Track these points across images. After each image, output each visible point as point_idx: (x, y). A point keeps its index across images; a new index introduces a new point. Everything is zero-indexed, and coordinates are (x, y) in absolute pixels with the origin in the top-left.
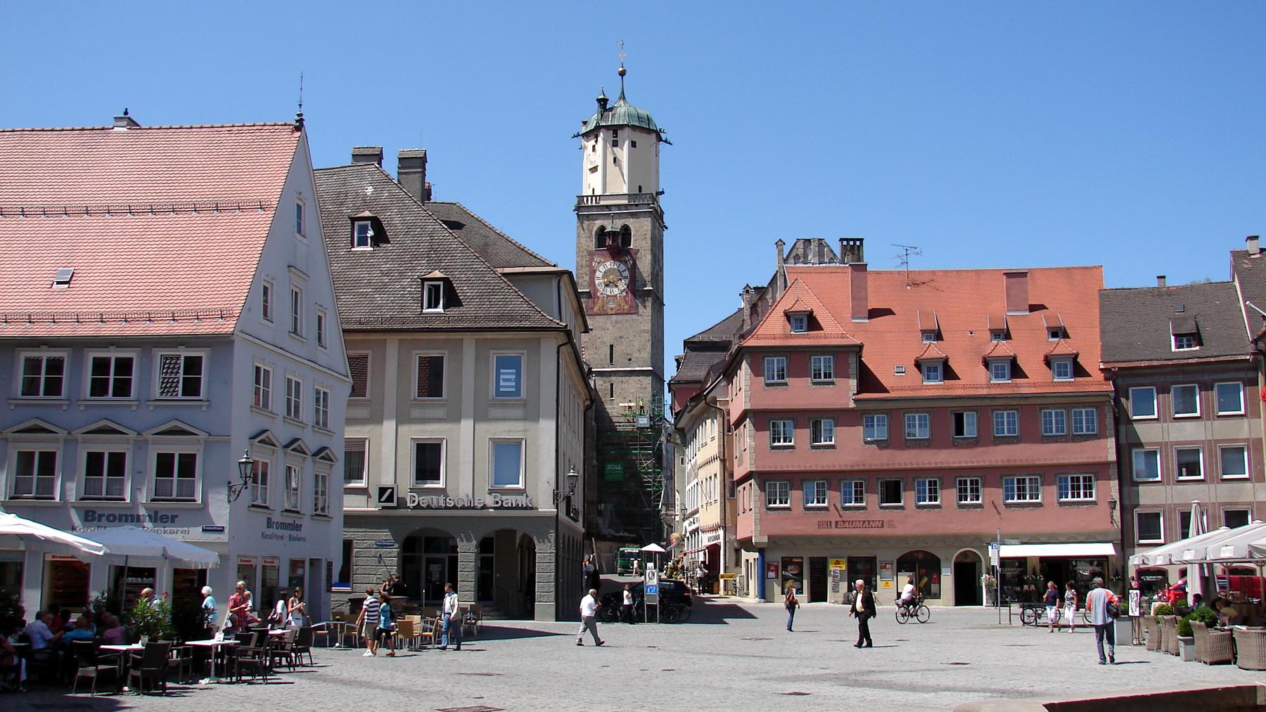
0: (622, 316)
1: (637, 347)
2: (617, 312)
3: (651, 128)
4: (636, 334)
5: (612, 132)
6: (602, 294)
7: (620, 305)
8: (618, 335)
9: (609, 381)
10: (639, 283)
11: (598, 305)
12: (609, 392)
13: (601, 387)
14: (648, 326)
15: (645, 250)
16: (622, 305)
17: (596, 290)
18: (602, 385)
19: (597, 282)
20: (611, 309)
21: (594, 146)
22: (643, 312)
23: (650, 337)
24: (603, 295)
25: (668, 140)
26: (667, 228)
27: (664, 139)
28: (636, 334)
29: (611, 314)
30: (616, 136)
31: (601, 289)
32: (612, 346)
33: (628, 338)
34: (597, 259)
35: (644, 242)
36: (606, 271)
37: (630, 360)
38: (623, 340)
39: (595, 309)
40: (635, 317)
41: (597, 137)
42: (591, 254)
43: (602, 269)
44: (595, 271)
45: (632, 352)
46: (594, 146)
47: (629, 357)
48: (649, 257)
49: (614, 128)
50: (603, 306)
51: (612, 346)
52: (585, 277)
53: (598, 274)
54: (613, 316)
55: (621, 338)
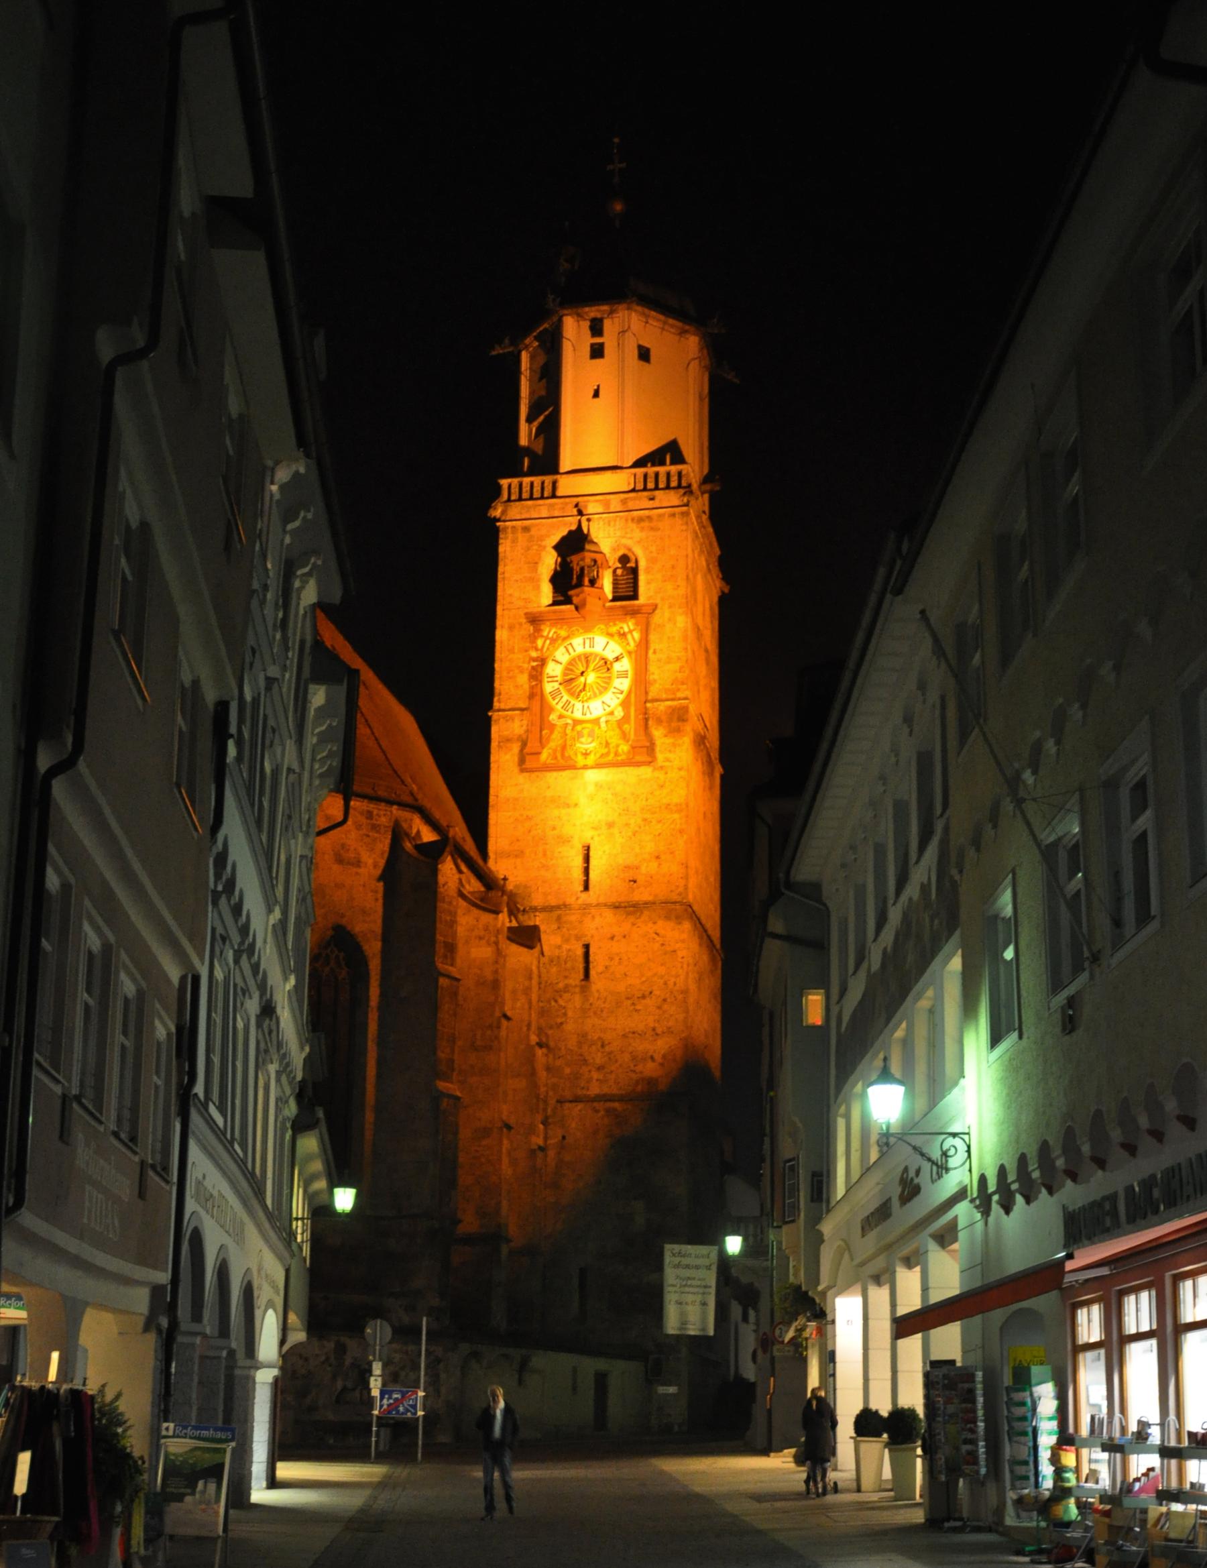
5: (586, 325)
6: (561, 717)
7: (607, 744)
9: (578, 938)
10: (657, 686)
11: (552, 744)
13: (557, 952)
17: (545, 709)
18: (559, 947)
19: (549, 687)
20: (586, 754)
22: (667, 760)
24: (562, 721)
29: (585, 767)
34: (548, 631)
36: (574, 660)
39: (545, 755)
43: (562, 655)
44: (543, 662)
50: (564, 748)
53: (553, 670)
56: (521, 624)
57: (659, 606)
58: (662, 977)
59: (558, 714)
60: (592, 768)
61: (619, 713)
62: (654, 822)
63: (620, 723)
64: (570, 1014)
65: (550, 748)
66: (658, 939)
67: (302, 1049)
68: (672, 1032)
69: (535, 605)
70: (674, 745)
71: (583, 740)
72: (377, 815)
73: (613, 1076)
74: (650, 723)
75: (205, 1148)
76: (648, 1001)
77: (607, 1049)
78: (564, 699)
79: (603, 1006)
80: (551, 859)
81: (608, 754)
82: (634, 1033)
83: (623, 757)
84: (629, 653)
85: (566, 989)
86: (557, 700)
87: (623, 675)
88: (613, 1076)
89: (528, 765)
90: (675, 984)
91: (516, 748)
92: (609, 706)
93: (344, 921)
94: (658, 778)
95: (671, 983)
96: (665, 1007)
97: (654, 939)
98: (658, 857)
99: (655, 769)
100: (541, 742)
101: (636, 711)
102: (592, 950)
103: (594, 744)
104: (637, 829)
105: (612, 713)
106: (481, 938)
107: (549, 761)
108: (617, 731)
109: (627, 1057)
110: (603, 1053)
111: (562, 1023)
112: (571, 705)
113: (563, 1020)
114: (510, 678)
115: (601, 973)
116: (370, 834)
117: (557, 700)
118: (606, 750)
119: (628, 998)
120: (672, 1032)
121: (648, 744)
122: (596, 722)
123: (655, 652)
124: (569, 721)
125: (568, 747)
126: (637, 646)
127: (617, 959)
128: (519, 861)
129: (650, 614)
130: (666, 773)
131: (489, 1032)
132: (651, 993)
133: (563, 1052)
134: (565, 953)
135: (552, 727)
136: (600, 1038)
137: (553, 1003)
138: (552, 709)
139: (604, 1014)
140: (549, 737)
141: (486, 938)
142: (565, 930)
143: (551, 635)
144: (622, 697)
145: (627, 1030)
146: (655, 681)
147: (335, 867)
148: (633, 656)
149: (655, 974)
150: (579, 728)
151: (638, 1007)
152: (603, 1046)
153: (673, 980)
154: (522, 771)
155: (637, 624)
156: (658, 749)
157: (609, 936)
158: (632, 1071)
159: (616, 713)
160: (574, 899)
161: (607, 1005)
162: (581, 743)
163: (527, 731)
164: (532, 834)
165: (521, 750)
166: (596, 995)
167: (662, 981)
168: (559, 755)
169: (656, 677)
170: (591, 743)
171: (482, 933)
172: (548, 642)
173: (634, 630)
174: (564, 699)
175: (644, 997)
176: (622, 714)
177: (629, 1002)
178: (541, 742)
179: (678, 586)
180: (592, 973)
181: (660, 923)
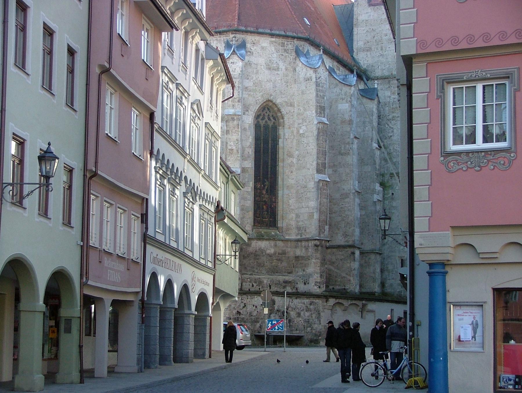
18: (390, 97)
64: (395, 131)
72: (287, 44)
80: (385, 52)
85: (393, 118)
93: (271, 98)
106: (343, 99)
111: (391, 136)
113: (392, 134)
116: (283, 54)
128: (368, 53)
137: (387, 126)
141: (346, 99)
142: (392, 88)
147: (267, 72)
164: (375, 38)
171: (343, 97)
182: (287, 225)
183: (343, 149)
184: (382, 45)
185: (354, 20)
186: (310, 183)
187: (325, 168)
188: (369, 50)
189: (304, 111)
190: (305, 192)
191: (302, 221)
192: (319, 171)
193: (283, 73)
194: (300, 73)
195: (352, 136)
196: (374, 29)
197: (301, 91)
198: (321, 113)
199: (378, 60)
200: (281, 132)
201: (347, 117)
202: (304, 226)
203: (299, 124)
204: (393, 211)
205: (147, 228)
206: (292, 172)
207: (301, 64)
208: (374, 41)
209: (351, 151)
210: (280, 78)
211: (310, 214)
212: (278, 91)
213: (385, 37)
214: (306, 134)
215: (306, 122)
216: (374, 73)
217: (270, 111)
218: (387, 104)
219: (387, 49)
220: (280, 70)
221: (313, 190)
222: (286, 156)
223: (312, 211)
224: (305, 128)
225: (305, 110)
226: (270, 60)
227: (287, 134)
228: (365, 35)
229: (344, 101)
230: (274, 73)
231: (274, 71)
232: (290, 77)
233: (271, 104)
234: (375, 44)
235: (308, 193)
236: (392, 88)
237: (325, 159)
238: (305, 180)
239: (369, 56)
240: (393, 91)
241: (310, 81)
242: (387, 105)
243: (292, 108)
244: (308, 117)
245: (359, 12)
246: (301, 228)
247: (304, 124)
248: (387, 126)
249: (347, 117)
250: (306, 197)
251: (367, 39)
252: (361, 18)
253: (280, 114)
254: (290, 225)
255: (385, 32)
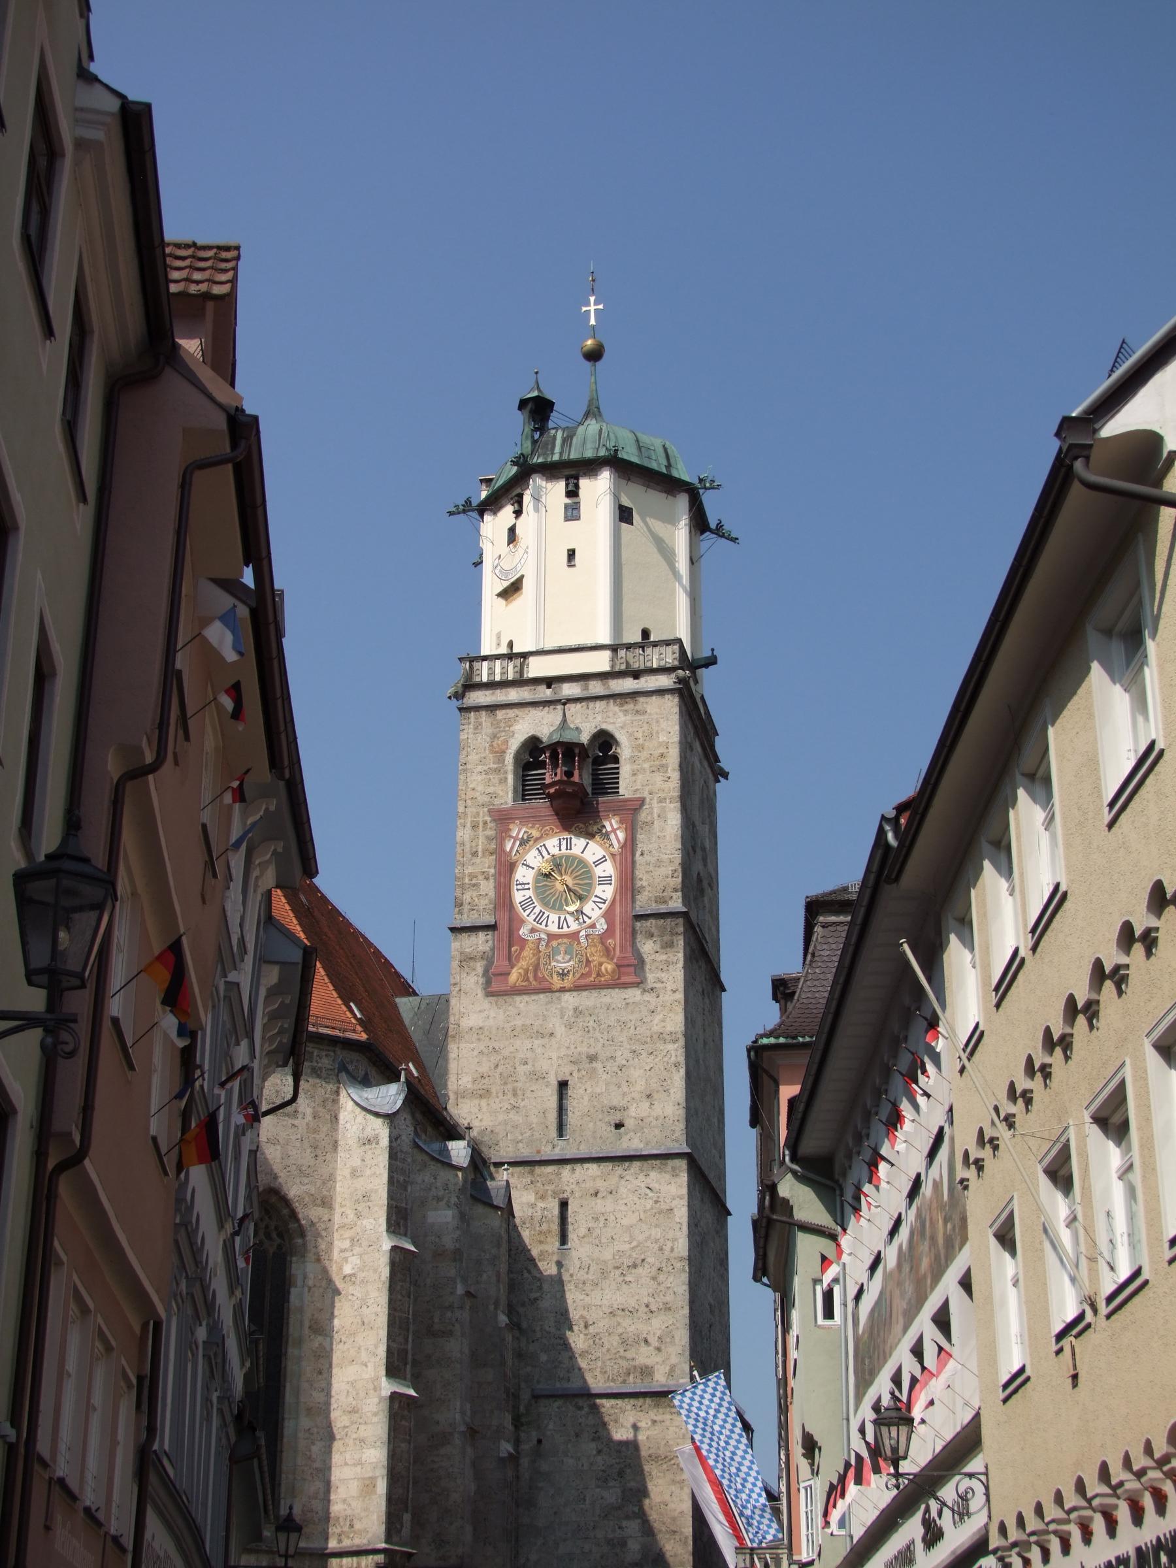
0: (595, 993)
1: (640, 1086)
2: (583, 982)
3: (675, 474)
4: (638, 1047)
8: (583, 1049)
11: (523, 963)
12: (555, 1227)
13: (529, 1212)
14: (675, 1021)
15: (661, 800)
16: (596, 959)
17: (515, 921)
18: (533, 1206)
19: (518, 897)
20: (563, 975)
21: (512, 530)
23: (681, 1052)
24: (536, 936)
25: (726, 527)
26: (725, 775)
27: (713, 526)
28: (638, 1047)
29: (563, 990)
30: (573, 493)
31: (529, 918)
32: (563, 1085)
33: (613, 1058)
34: (518, 831)
35: (658, 778)
37: (619, 1126)
38: (598, 1065)
39: (514, 976)
40: (634, 994)
41: (519, 500)
42: (502, 819)
43: (534, 859)
44: (511, 867)
45: (623, 1103)
46: (512, 530)
47: (617, 1117)
48: (674, 819)
49: (567, 472)
50: (537, 967)
51: (563, 1085)
52: (483, 883)
53: (523, 875)
54: (567, 996)
55: (592, 1058)
56: (485, 823)
57: (648, 800)
58: (657, 1241)
59: (530, 927)
60: (570, 990)
61: (602, 926)
62: (645, 1054)
63: (603, 937)
65: (521, 968)
66: (651, 1194)
67: (243, 1364)
68: (670, 1309)
69: (503, 801)
70: (667, 963)
71: (559, 958)
72: (318, 1056)
73: (599, 1364)
74: (639, 937)
75: (160, 1514)
76: (640, 1270)
77: (591, 1329)
78: (537, 910)
79: (586, 1276)
80: (523, 1100)
81: (589, 974)
82: (623, 1310)
83: (608, 977)
84: (613, 855)
86: (528, 912)
87: (606, 881)
88: (599, 1364)
89: (495, 987)
90: (672, 1250)
91: (479, 967)
92: (590, 918)
94: (649, 1002)
95: (667, 1248)
96: (661, 1278)
97: (647, 1195)
98: (649, 1096)
99: (644, 990)
100: (510, 959)
101: (621, 923)
102: (571, 1208)
103: (571, 963)
104: (624, 1062)
105: (593, 926)
106: (439, 1199)
107: (519, 983)
108: (600, 947)
109: (615, 1341)
110: (586, 1335)
111: (536, 1299)
112: (545, 916)
113: (538, 1294)
114: (474, 885)
115: (584, 1237)
117: (528, 912)
118: (587, 969)
119: (618, 1268)
120: (670, 1309)
121: (636, 962)
122: (575, 936)
123: (642, 854)
124: (543, 936)
125: (542, 965)
126: (622, 848)
127: (602, 1219)
128: (484, 1102)
129: (635, 810)
130: (658, 996)
131: (449, 1314)
132: (643, 1260)
133: (538, 1335)
134: (539, 1213)
135: (523, 942)
136: (582, 1317)
137: (526, 1275)
138: (522, 922)
139: (588, 1288)
140: (520, 953)
141: (446, 1199)
142: (539, 1185)
143: (520, 836)
144: (604, 907)
145: (615, 1306)
146: (642, 887)
148: (618, 858)
149: (649, 1238)
150: (554, 943)
151: (628, 1279)
152: (586, 1327)
153: (669, 1244)
154: (489, 994)
155: (621, 822)
156: (648, 967)
157: (592, 1191)
158: (620, 1357)
159: (598, 926)
160: (550, 1147)
161: (590, 1277)
162: (558, 962)
163: (493, 949)
165: (486, 972)
166: (578, 1264)
167: (656, 1247)
168: (531, 976)
169: (645, 883)
170: (568, 962)
171: (441, 1193)
172: (518, 843)
173: (617, 829)
174: (537, 910)
175: (635, 1266)
176: (605, 927)
177: (618, 1272)
178: (510, 959)
179: (669, 778)
180: (572, 1236)
181: (653, 1175)
182: (303, 1511)
183: (436, 1320)
184: (516, 1084)
185: (451, 1026)
186: (368, 1401)
187: (406, 1364)
188: (485, 1094)
189: (355, 1219)
190: (352, 1423)
191: (344, 1501)
192: (392, 1371)
193: (307, 1124)
194: (348, 1126)
195: (460, 1290)
196: (497, 1048)
197: (349, 1170)
198: (398, 1224)
199: (506, 1118)
200: (296, 1269)
201: (448, 1242)
202: (349, 1512)
203: (342, 1251)
204: (540, 1485)
205: (151, 1430)
206: (320, 1373)
207: (351, 1103)
208: (497, 1075)
209: (457, 1326)
210: (299, 1136)
211: (367, 1482)
212: (294, 1167)
213: (523, 1067)
214: (361, 1275)
215: (360, 1246)
216: (497, 1148)
217: (270, 1218)
218: (527, 1222)
219: (528, 1094)
220: (300, 1116)
221: (375, 1419)
222: (306, 1331)
223: (370, 1474)
224: (358, 1262)
225: (359, 1216)
226: (277, 1091)
227: (311, 1276)
228: (477, 1060)
229: (442, 1203)
230: (285, 1123)
231: (287, 1118)
232: (322, 1135)
233: (274, 1199)
234: (498, 1081)
235: (362, 1428)
236: (539, 1185)
237: (407, 1340)
238: (355, 1393)
239: (484, 1109)
240: (541, 1193)
241: (374, 1144)
242: (528, 1225)
243: (326, 1211)
244: (368, 1232)
245: (462, 1010)
246: (341, 1520)
247: (355, 1252)
248: (526, 1275)
249: (448, 1242)
250: (354, 1436)
251: (481, 1070)
252: (466, 1023)
253: (296, 1225)
254: (311, 1511)
255: (522, 1056)
